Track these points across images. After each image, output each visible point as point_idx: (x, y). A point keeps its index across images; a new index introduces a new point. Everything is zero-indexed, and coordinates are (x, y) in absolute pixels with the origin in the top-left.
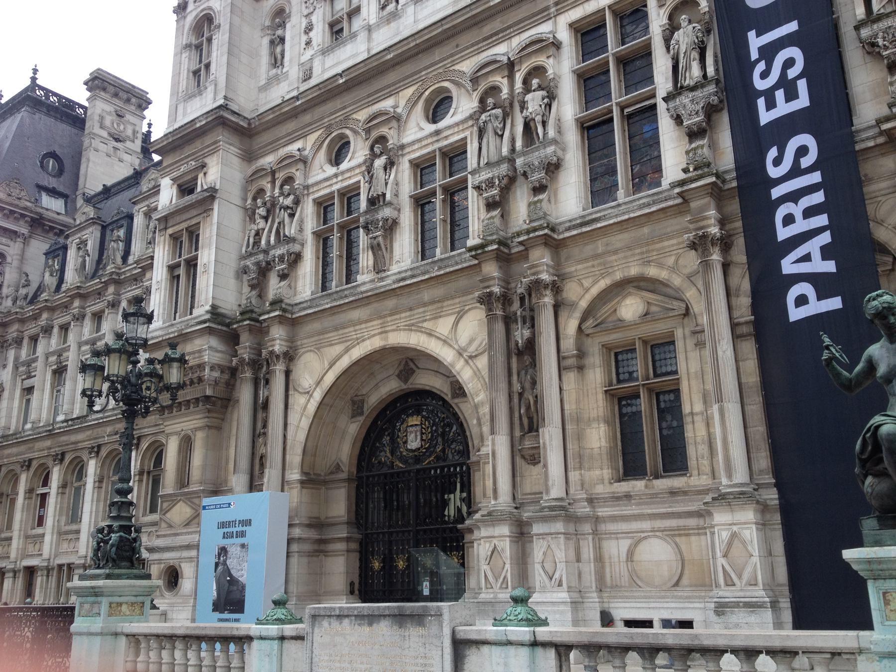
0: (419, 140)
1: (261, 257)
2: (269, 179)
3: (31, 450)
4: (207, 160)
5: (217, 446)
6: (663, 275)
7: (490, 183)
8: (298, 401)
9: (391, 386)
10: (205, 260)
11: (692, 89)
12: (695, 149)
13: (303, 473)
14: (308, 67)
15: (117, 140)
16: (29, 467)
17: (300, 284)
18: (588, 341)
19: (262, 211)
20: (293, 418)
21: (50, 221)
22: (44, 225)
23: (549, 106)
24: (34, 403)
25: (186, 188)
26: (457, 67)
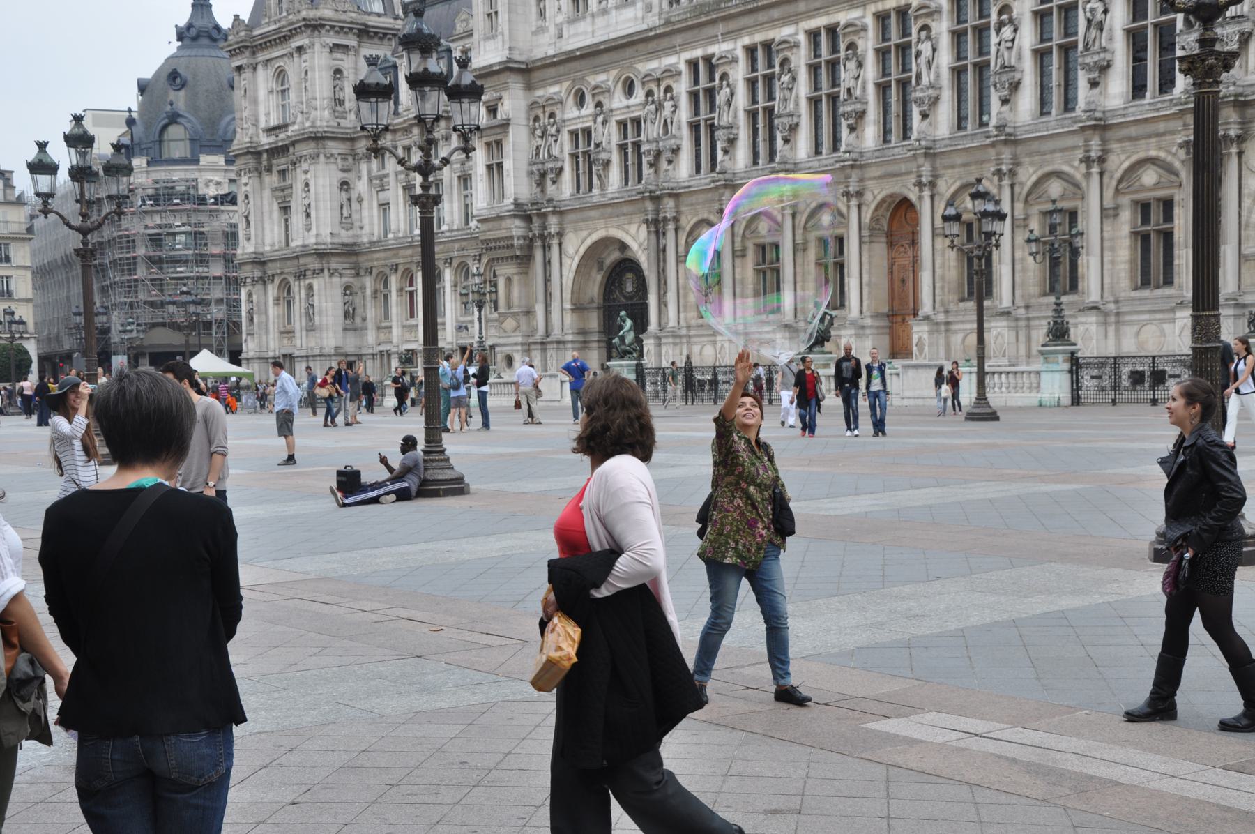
0: (620, 109)
1: (540, 166)
2: (542, 110)
3: (396, 256)
5: (526, 285)
8: (566, 261)
9: (614, 256)
13: (572, 304)
16: (396, 270)
17: (563, 187)
19: (538, 132)
20: (565, 272)
21: (373, 27)
22: (369, 32)
23: (674, 111)
24: (393, 216)
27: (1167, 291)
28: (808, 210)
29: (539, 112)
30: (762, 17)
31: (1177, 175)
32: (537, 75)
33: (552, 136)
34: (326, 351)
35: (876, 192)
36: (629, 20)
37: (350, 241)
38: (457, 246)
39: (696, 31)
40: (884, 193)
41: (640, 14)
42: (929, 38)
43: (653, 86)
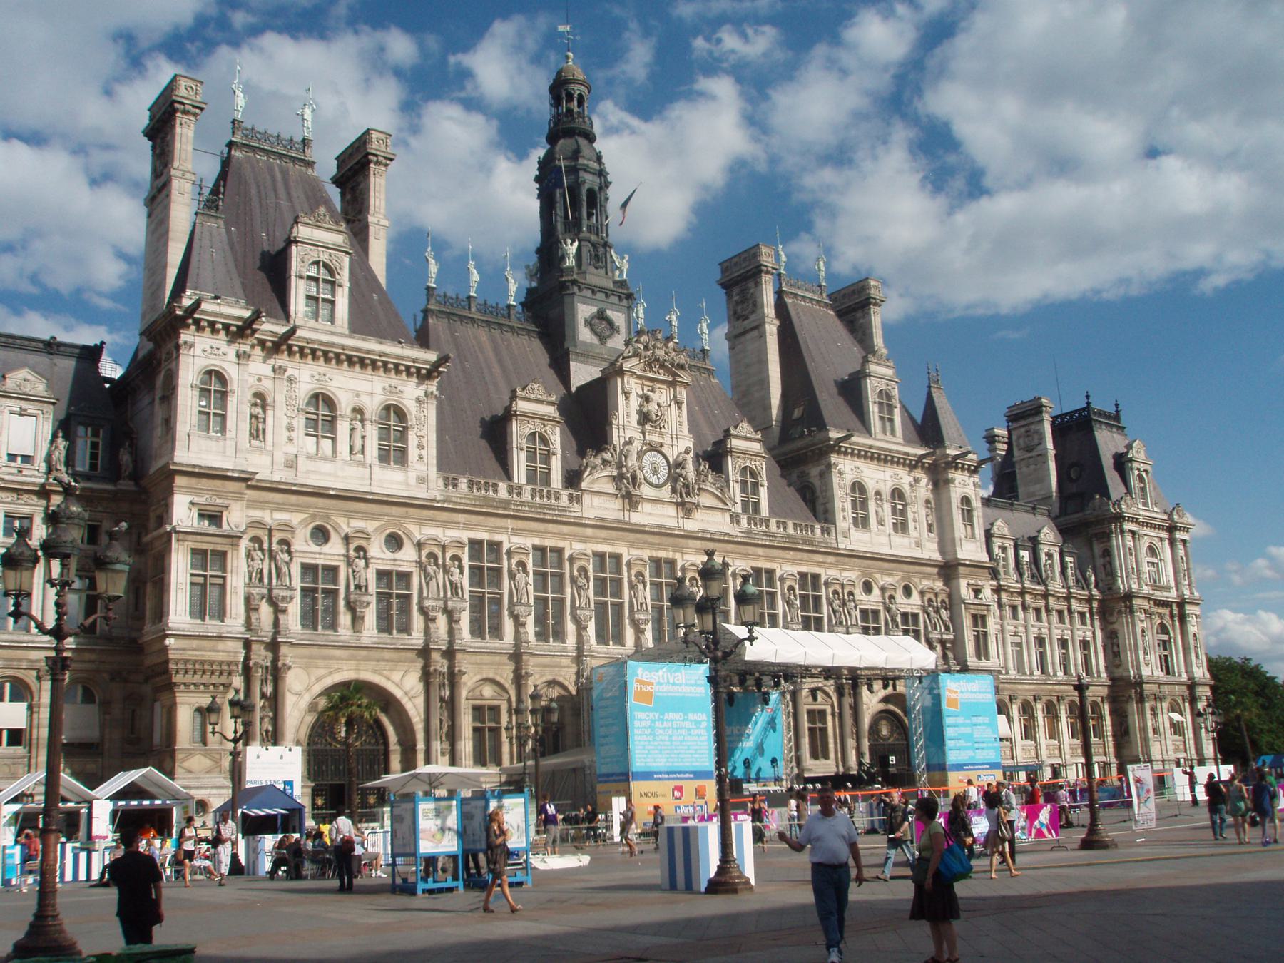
2: (267, 533)
7: (433, 608)
14: (292, 457)
26: (407, 526)
27: (827, 762)
30: (551, 527)
31: (831, 698)
39: (481, 518)
41: (413, 481)
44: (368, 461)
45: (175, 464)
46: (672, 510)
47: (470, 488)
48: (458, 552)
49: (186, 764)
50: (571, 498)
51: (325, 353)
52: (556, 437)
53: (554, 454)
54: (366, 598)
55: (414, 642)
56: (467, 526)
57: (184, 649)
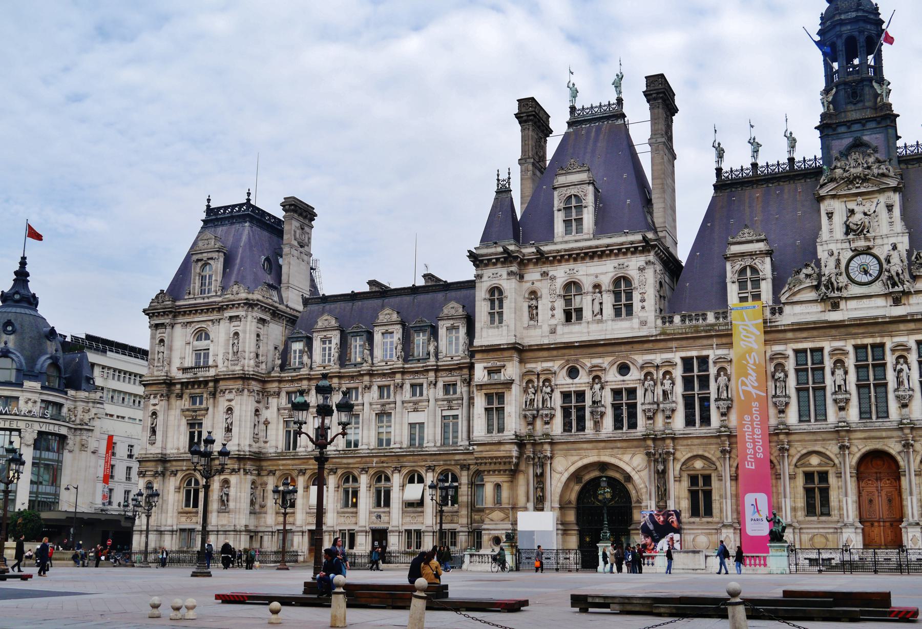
3: (304, 463)
4: (505, 363)
6: (710, 456)
7: (649, 410)
8: (556, 476)
9: (595, 474)
10: (509, 411)
11: (724, 400)
12: (723, 420)
15: (302, 246)
16: (304, 474)
17: (554, 427)
18: (682, 473)
25: (491, 371)
28: (799, 455)
29: (534, 378)
32: (531, 354)
33: (548, 393)
34: (238, 528)
35: (860, 447)
36: (626, 329)
37: (257, 450)
38: (375, 460)
39: (691, 341)
40: (867, 448)
42: (906, 362)
43: (652, 370)
44: (604, 318)
45: (476, 347)
46: (881, 302)
47: (683, 321)
48: (670, 369)
49: (490, 516)
50: (773, 312)
51: (570, 255)
52: (766, 267)
53: (763, 280)
54: (599, 409)
55: (639, 434)
56: (678, 349)
57: (481, 452)
